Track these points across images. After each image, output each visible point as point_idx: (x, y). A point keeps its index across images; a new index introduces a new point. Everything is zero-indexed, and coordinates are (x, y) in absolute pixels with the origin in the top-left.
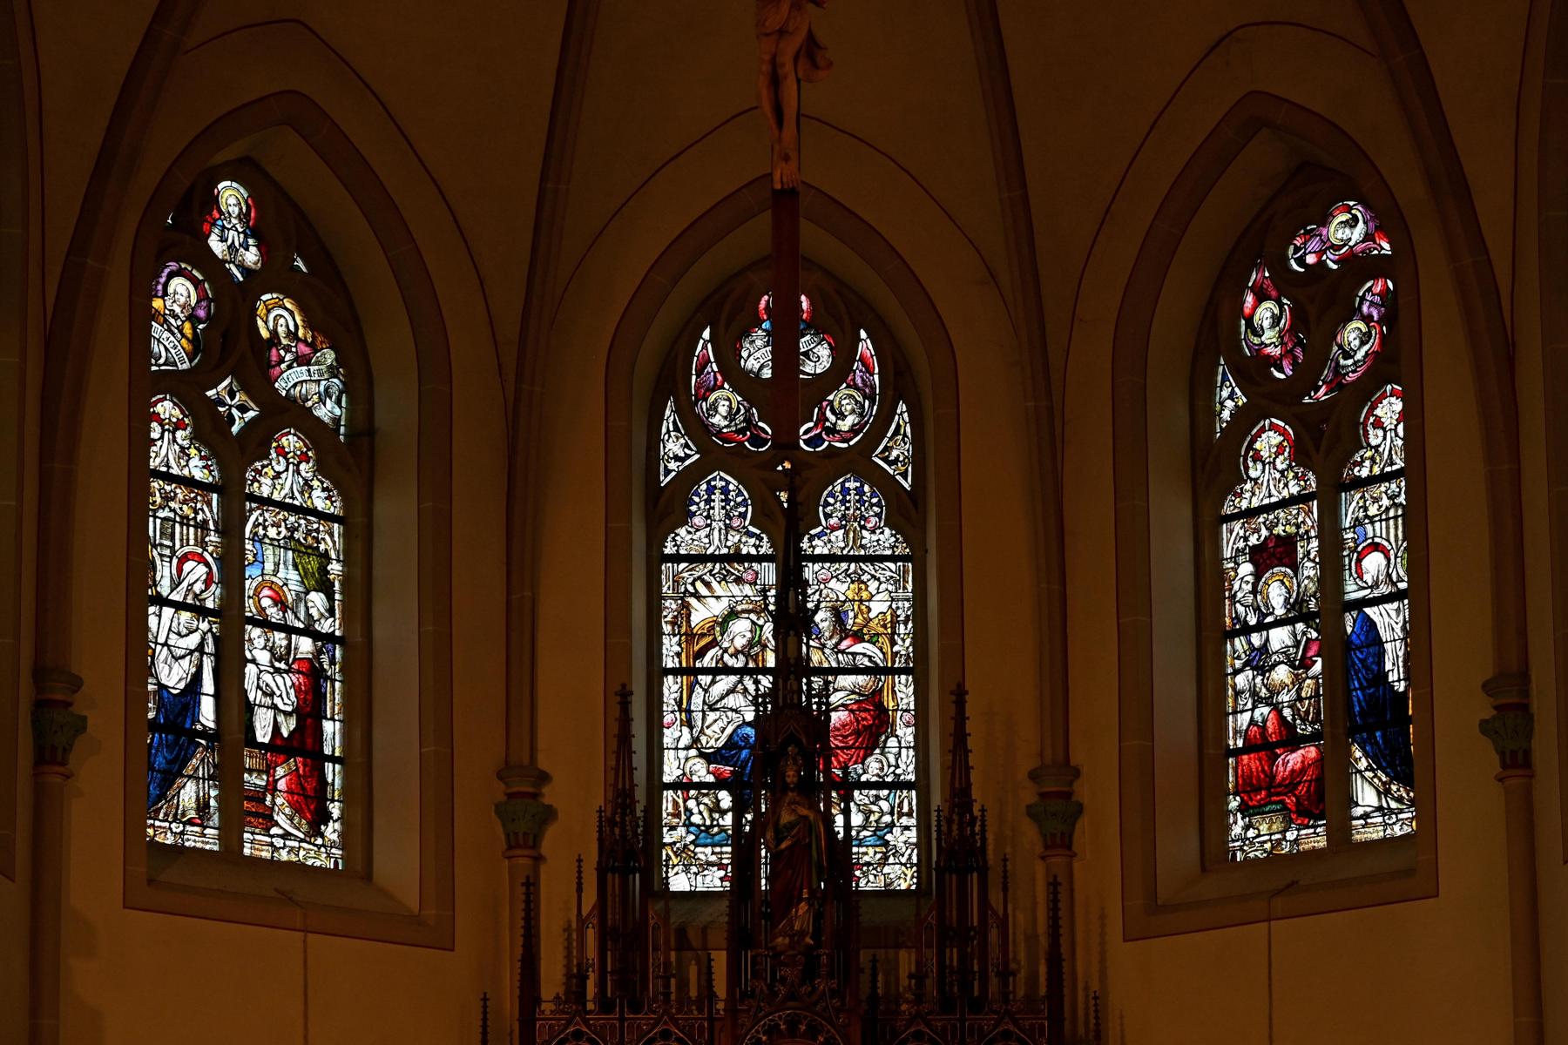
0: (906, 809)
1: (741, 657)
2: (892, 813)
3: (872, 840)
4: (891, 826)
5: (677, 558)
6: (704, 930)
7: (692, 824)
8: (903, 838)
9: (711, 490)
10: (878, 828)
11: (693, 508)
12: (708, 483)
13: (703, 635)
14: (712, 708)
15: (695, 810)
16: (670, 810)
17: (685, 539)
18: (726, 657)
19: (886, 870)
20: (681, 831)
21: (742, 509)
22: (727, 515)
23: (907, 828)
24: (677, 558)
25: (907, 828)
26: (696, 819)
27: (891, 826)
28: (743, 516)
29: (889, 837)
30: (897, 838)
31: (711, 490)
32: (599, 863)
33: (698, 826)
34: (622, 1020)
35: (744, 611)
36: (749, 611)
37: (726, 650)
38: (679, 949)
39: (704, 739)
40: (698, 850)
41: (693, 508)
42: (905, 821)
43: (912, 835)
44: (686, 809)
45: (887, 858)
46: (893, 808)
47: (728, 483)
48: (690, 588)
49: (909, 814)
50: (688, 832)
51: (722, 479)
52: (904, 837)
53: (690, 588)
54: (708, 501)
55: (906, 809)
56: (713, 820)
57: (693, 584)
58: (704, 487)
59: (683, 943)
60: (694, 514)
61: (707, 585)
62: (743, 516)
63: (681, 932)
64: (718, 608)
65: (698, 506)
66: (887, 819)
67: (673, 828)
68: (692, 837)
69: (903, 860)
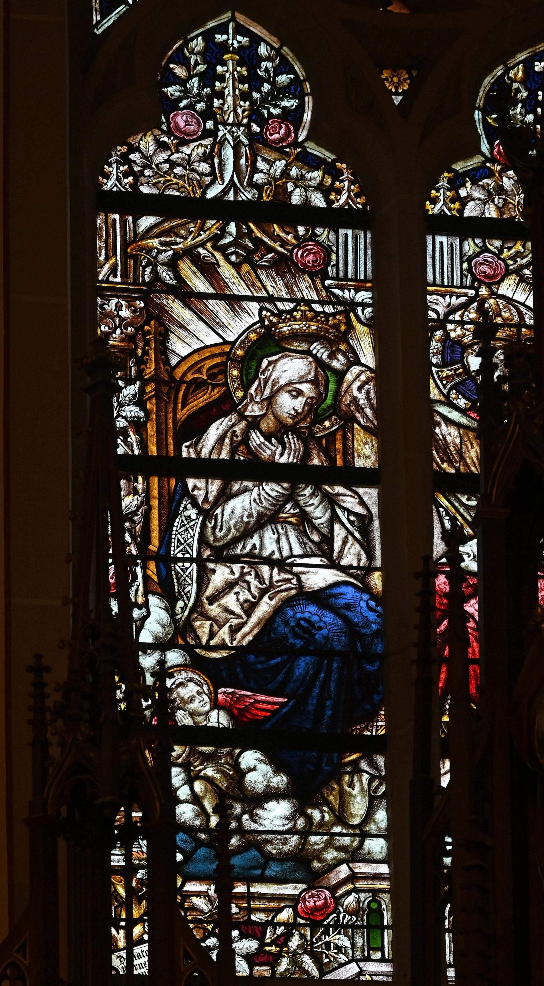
1: (292, 441)
5: (132, 203)
9: (214, 53)
11: (173, 91)
12: (208, 36)
13: (198, 386)
14: (222, 556)
17: (152, 159)
18: (256, 438)
21: (290, 103)
22: (255, 114)
24: (132, 203)
28: (293, 117)
31: (214, 53)
35: (295, 336)
36: (310, 338)
37: (254, 423)
39: (203, 628)
41: (173, 91)
47: (256, 40)
48: (165, 274)
51: (240, 30)
53: (165, 274)
54: (209, 78)
57: (172, 265)
58: (199, 44)
60: (173, 105)
61: (209, 270)
62: (293, 117)
64: (237, 325)
65: (183, 83)
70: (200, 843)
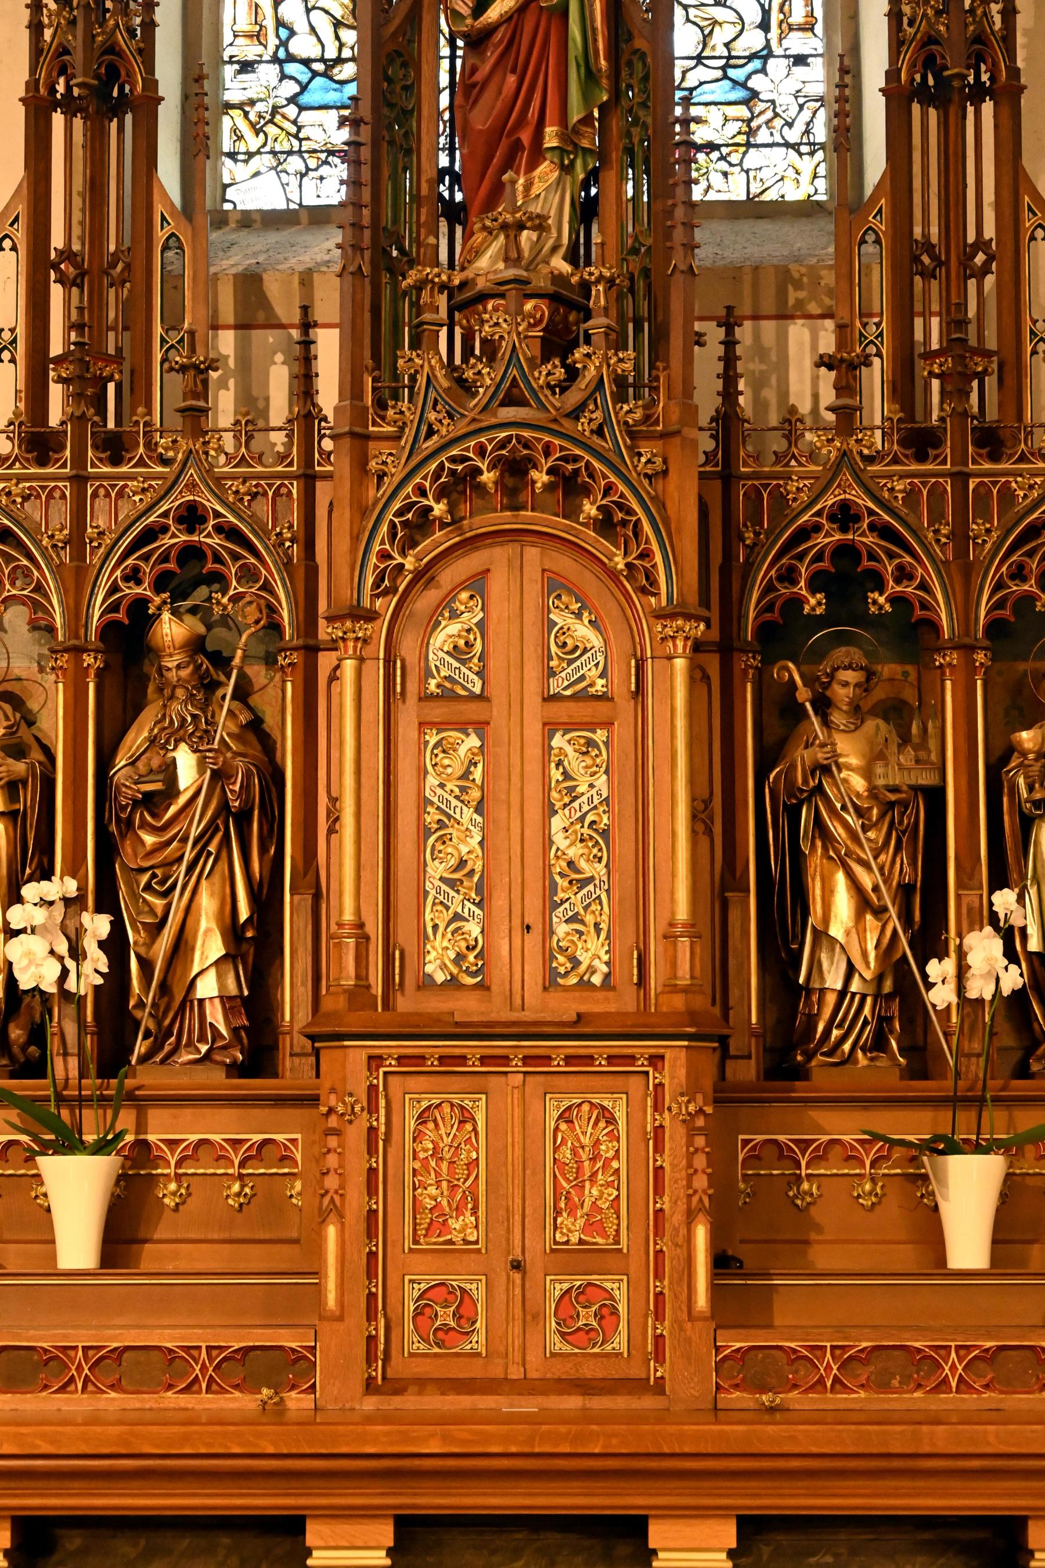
0: (798, 16)
2: (764, 26)
3: (722, 91)
4: (765, 55)
6: (306, 279)
7: (291, 58)
8: (791, 85)
10: (730, 61)
15: (301, 26)
16: (244, 23)
19: (754, 158)
20: (268, 73)
23: (800, 60)
25: (800, 60)
26: (303, 46)
27: (765, 55)
29: (757, 82)
30: (778, 83)
32: (32, 85)
33: (306, 62)
34: (79, 480)
38: (242, 326)
40: (306, 117)
42: (797, 42)
43: (816, 77)
44: (280, 23)
45: (751, 132)
46: (766, 13)
49: (808, 27)
50: (283, 77)
52: (795, 86)
55: (798, 16)
56: (341, 46)
59: (253, 311)
63: (250, 284)
66: (753, 40)
67: (246, 66)
68: (290, 88)
69: (793, 135)
70: (315, 74)
